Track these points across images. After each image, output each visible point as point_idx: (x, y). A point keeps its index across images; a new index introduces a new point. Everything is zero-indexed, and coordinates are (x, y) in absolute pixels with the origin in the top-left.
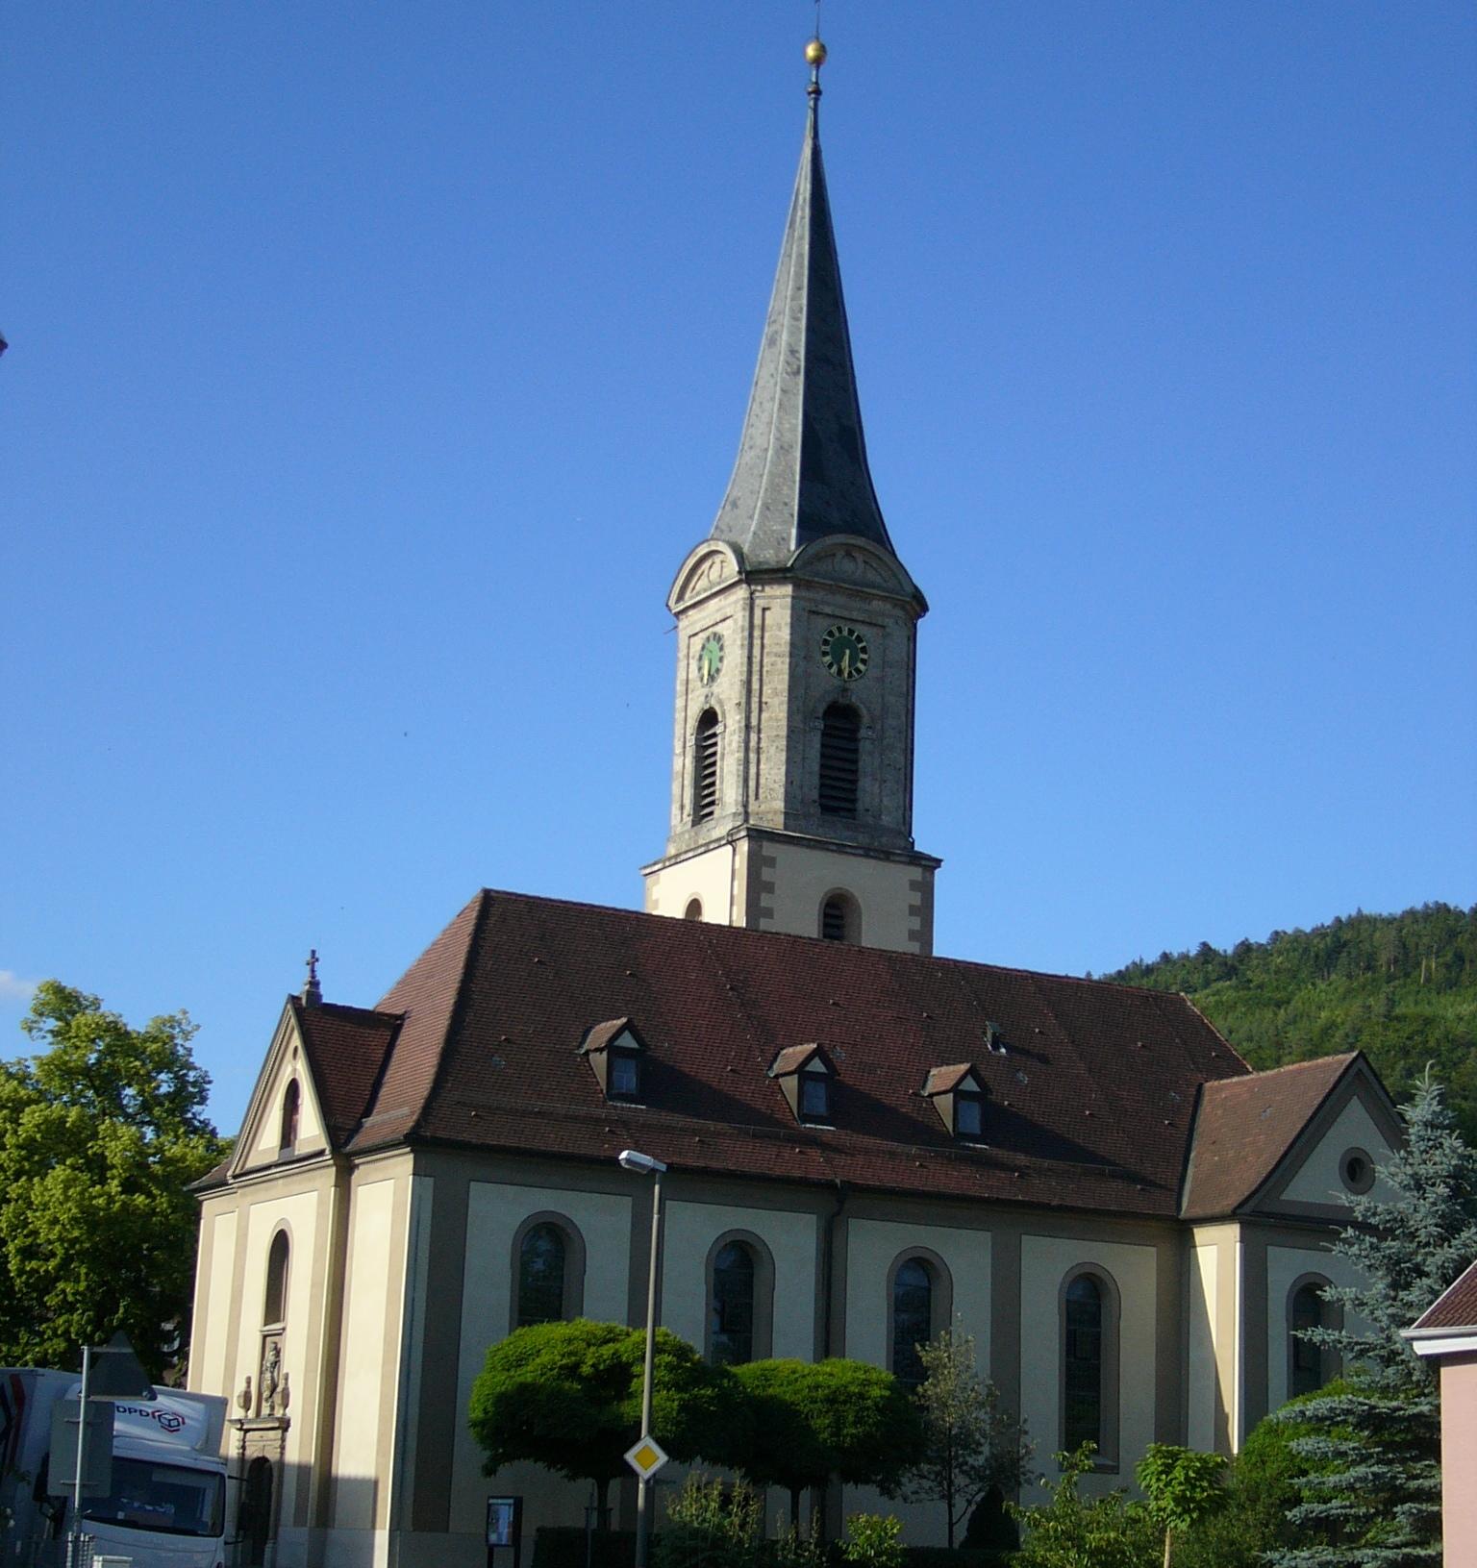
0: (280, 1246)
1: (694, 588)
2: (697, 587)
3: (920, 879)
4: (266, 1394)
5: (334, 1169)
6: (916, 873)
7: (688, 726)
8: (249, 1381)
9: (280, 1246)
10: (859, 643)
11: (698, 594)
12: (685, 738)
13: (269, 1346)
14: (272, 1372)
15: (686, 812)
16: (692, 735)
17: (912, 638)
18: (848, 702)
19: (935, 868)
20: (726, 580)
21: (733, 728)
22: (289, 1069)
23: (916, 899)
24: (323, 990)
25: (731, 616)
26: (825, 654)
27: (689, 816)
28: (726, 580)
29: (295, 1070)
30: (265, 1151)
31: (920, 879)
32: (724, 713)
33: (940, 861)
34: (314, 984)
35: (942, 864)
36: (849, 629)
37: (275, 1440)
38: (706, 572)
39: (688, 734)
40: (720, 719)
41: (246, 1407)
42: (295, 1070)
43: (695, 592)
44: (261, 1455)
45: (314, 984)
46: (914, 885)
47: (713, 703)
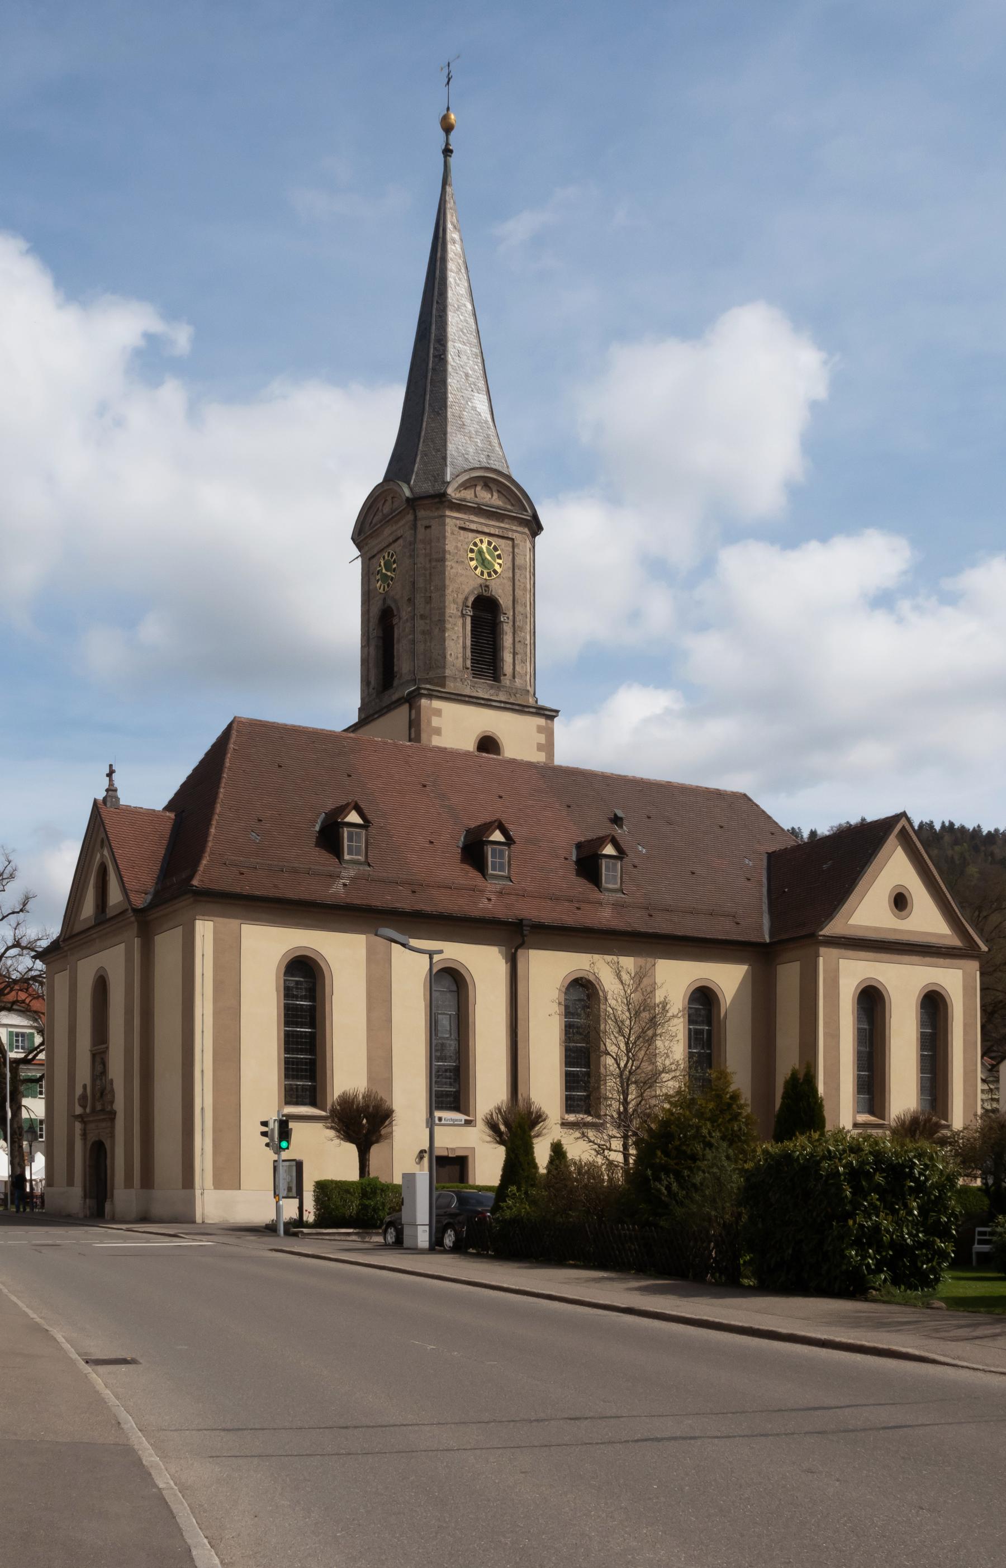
0: (101, 986)
1: (371, 522)
2: (374, 522)
3: (544, 724)
4: (98, 1095)
5: (136, 924)
6: (541, 721)
7: (371, 624)
8: (85, 1087)
9: (101, 986)
10: (495, 551)
11: (376, 525)
12: (368, 633)
13: (98, 1059)
14: (101, 1080)
15: (371, 687)
16: (374, 630)
17: (532, 549)
18: (489, 595)
19: (555, 717)
20: (397, 509)
21: (405, 618)
22: (99, 856)
23: (542, 739)
24: (120, 794)
25: (402, 536)
26: (472, 559)
27: (374, 689)
28: (397, 509)
29: (102, 855)
30: (85, 920)
31: (544, 724)
32: (398, 609)
33: (557, 711)
34: (111, 790)
35: (560, 713)
36: (488, 541)
37: (30, 1002)
38: (380, 509)
39: (371, 630)
40: (395, 613)
41: (84, 1107)
42: (102, 855)
43: (372, 525)
44: (97, 1139)
45: (111, 790)
46: (540, 729)
47: (389, 602)
